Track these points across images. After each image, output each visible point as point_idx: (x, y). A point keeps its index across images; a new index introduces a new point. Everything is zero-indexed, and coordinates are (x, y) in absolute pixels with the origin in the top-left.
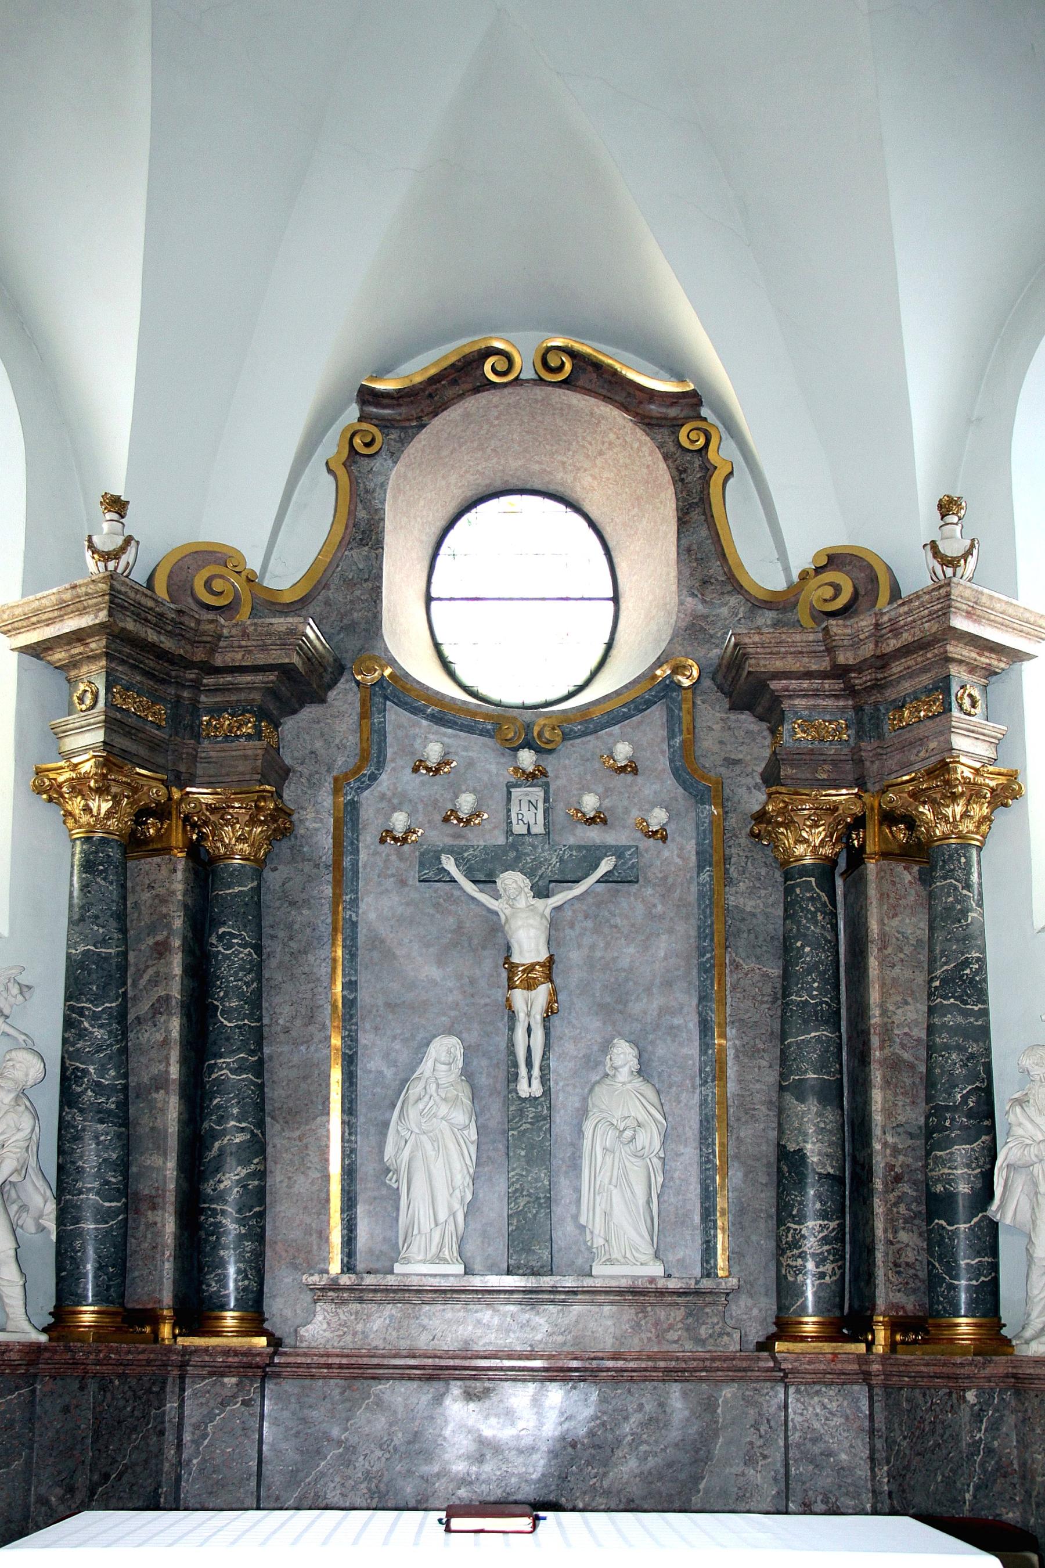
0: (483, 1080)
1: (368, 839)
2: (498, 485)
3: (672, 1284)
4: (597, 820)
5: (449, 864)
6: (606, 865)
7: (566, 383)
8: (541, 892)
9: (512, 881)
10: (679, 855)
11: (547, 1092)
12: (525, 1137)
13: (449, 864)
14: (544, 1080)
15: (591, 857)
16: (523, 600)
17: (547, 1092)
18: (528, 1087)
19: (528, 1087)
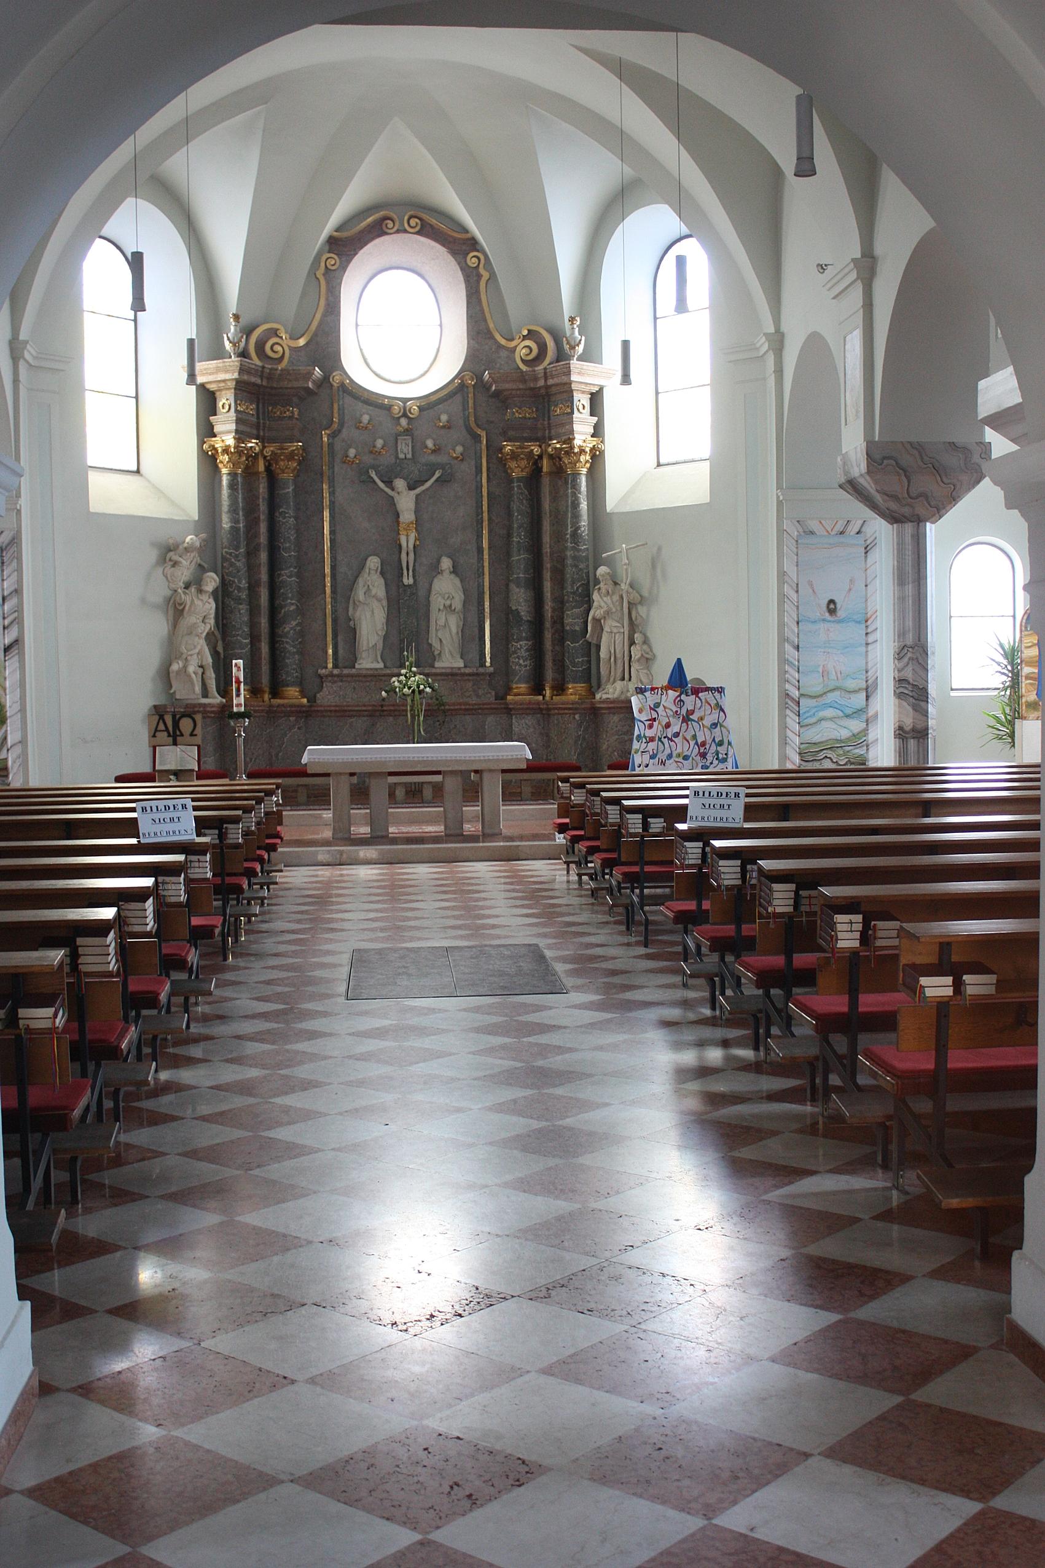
1: (338, 460)
2: (388, 266)
3: (467, 671)
5: (373, 475)
6: (437, 475)
7: (418, 233)
9: (400, 484)
13: (373, 475)
14: (414, 577)
15: (431, 469)
16: (401, 335)
18: (408, 580)
19: (408, 580)
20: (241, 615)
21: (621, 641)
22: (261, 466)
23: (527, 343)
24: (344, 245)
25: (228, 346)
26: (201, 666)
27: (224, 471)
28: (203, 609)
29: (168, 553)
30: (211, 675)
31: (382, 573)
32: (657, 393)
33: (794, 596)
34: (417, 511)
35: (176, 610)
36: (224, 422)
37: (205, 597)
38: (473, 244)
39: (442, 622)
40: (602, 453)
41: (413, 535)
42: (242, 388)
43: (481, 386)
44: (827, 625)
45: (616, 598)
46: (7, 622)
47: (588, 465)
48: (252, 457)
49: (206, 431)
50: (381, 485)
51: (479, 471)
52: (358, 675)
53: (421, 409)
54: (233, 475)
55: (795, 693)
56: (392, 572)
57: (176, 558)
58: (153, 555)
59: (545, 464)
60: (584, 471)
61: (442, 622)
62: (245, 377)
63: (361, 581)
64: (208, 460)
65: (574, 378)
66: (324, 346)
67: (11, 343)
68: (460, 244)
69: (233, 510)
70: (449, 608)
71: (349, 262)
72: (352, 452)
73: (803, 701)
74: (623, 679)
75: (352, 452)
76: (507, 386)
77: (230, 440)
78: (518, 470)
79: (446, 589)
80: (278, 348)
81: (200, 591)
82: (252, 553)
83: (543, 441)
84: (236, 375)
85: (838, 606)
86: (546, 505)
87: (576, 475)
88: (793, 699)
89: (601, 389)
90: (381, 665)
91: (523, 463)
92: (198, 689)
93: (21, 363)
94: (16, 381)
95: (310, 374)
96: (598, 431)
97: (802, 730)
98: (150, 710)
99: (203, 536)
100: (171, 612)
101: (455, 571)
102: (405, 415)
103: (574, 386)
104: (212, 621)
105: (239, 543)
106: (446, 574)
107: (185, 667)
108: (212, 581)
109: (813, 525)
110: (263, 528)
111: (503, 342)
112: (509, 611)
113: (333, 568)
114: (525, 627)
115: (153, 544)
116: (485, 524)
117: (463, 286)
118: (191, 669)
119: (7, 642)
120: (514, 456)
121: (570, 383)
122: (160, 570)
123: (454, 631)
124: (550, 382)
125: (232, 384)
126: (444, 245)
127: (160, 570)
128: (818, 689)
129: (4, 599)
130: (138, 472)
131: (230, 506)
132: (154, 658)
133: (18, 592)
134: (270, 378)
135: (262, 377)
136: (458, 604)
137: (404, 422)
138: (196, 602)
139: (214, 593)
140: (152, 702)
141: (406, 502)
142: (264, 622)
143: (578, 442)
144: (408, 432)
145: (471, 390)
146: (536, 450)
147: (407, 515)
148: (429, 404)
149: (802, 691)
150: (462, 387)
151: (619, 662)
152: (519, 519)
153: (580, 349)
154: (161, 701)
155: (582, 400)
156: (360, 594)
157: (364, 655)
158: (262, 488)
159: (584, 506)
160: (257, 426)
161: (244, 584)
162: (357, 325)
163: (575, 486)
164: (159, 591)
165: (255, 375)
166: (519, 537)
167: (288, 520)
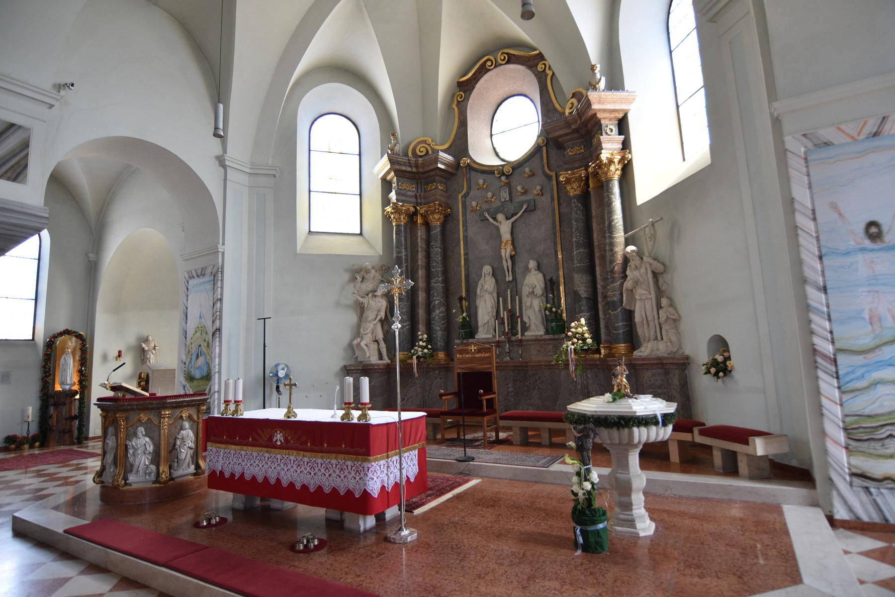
1: (468, 211)
2: (505, 96)
3: (547, 337)
4: (525, 192)
7: (508, 63)
8: (507, 218)
9: (500, 217)
10: (544, 201)
11: (514, 279)
17: (514, 279)
21: (650, 305)
22: (420, 220)
24: (465, 87)
26: (377, 341)
29: (357, 273)
30: (383, 345)
32: (678, 107)
33: (811, 225)
34: (512, 233)
35: (361, 309)
37: (377, 299)
38: (541, 57)
39: (528, 304)
40: (630, 161)
41: (509, 248)
44: (869, 256)
45: (643, 270)
47: (619, 172)
49: (386, 201)
50: (491, 220)
54: (397, 226)
55: (829, 349)
58: (346, 277)
60: (616, 177)
61: (528, 304)
62: (397, 167)
64: (386, 218)
65: (595, 106)
66: (460, 146)
68: (532, 61)
71: (470, 94)
72: (474, 204)
73: (841, 359)
74: (656, 339)
76: (558, 134)
78: (574, 190)
79: (534, 281)
80: (422, 149)
85: (885, 228)
87: (609, 181)
88: (825, 357)
91: (575, 185)
93: (229, 171)
95: (436, 160)
96: (626, 145)
97: (845, 397)
100: (358, 309)
101: (539, 268)
102: (503, 174)
103: (599, 115)
104: (382, 314)
106: (533, 272)
109: (827, 134)
110: (421, 256)
112: (576, 294)
113: (467, 276)
114: (584, 302)
115: (346, 270)
116: (558, 234)
120: (568, 181)
123: (537, 309)
127: (352, 285)
128: (867, 341)
130: (361, 234)
133: (221, 300)
135: (411, 166)
136: (539, 290)
137: (503, 178)
138: (372, 303)
140: (343, 363)
141: (505, 228)
143: (604, 156)
145: (544, 148)
148: (517, 166)
149: (838, 345)
151: (651, 324)
153: (602, 85)
155: (609, 126)
157: (480, 329)
158: (421, 233)
160: (416, 196)
162: (491, 135)
164: (350, 295)
165: (405, 165)
167: (437, 250)
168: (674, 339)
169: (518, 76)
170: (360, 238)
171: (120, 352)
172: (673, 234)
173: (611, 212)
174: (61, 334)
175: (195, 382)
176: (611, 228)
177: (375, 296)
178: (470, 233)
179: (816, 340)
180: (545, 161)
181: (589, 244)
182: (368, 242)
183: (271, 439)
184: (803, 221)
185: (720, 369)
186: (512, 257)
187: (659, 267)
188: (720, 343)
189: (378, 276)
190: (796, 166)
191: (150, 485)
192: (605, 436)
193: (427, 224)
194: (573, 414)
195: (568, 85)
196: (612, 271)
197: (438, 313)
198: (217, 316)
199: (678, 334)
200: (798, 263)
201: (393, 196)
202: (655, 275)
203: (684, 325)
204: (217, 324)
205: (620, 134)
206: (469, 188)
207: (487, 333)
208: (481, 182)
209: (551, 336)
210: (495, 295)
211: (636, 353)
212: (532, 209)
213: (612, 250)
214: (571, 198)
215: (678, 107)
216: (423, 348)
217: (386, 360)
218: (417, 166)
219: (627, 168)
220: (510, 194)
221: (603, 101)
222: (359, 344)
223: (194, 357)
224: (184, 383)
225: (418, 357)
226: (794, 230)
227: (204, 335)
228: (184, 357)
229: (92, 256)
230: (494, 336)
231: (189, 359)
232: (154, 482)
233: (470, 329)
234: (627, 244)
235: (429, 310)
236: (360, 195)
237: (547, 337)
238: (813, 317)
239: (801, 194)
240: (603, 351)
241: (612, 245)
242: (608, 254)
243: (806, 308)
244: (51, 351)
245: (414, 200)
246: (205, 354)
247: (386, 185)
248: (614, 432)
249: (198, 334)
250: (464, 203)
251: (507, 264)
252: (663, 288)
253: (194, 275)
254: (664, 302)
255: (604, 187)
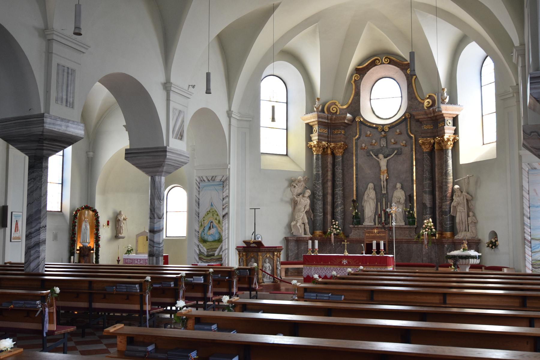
0: (377, 191)
1: (359, 148)
3: (406, 226)
4: (396, 143)
5: (371, 153)
7: (388, 64)
8: (385, 157)
9: (381, 156)
10: (407, 150)
11: (387, 192)
12: (383, 199)
13: (371, 153)
14: (387, 190)
15: (393, 150)
16: (384, 101)
17: (387, 192)
18: (384, 192)
20: (319, 205)
21: (464, 215)
22: (329, 152)
23: (428, 100)
24: (361, 71)
25: (315, 109)
26: (304, 223)
27: (315, 153)
28: (305, 202)
29: (292, 183)
30: (307, 226)
31: (375, 189)
32: (482, 116)
33: (527, 196)
35: (295, 204)
36: (315, 136)
37: (305, 199)
40: (458, 141)
41: (386, 175)
42: (320, 123)
43: (412, 116)
45: (462, 198)
46: (224, 207)
47: (452, 146)
48: (325, 149)
49: (309, 139)
50: (374, 157)
51: (412, 150)
52: (365, 228)
53: (389, 128)
54: (317, 155)
55: (529, 238)
56: (377, 189)
57: (295, 185)
58: (286, 184)
59: (436, 146)
60: (450, 148)
62: (320, 120)
63: (366, 193)
64: (309, 149)
66: (355, 107)
67: (227, 112)
69: (317, 167)
70: (399, 202)
71: (363, 77)
72: (363, 145)
73: (532, 241)
74: (466, 231)
75: (363, 145)
77: (315, 143)
78: (426, 149)
79: (399, 194)
80: (334, 109)
81: (304, 196)
82: (324, 184)
83: (434, 137)
84: (317, 119)
86: (437, 162)
87: (447, 150)
88: (528, 241)
89: (457, 116)
90: (373, 224)
91: (427, 146)
92: (302, 231)
93: (232, 120)
94: (230, 125)
95: (345, 118)
96: (456, 132)
97: (533, 254)
98: (283, 239)
99: (306, 177)
100: (293, 204)
101: (402, 188)
102: (383, 131)
103: (444, 115)
104: (308, 208)
105: (319, 179)
106: (399, 190)
107: (296, 223)
108: (308, 193)
110: (330, 174)
111: (420, 100)
113: (357, 188)
114: (428, 210)
115: (286, 180)
117: (406, 81)
118: (298, 224)
119: (224, 213)
120: (423, 143)
121: (443, 114)
122: (289, 189)
124: (436, 114)
125: (316, 123)
126: (398, 67)
129: (223, 199)
130: (287, 155)
131: (316, 166)
132: (285, 220)
133: (228, 196)
134: (331, 120)
135: (328, 119)
138: (302, 200)
139: (309, 197)
140: (284, 236)
141: (383, 163)
142: (329, 208)
143: (446, 137)
144: (385, 137)
145: (409, 120)
146: (432, 141)
147: (384, 167)
148: (392, 126)
149: (532, 237)
150: (405, 119)
151: (464, 223)
152: (427, 168)
153: (447, 100)
154: (288, 235)
155: (449, 121)
156: (365, 197)
157: (366, 220)
158: (330, 159)
159: (450, 162)
160: (328, 137)
161: (321, 194)
162: (370, 99)
163: (446, 154)
164: (288, 195)
166: (427, 175)
167: (339, 171)
168: (474, 231)
169: (393, 70)
170: (285, 158)
171: (108, 222)
172: (477, 183)
173: (447, 166)
174: (83, 209)
175: (208, 243)
176: (446, 174)
177: (304, 196)
178: (360, 162)
179: (526, 235)
180: (409, 127)
181: (432, 179)
182: (293, 161)
183: (341, 262)
184: (525, 194)
185: (493, 245)
186: (386, 180)
187: (469, 197)
188: (494, 234)
189: (304, 185)
190: (525, 174)
191: (271, 283)
192: (461, 261)
193: (333, 154)
194: (449, 256)
195: (426, 89)
196: (446, 196)
197: (339, 209)
198: (226, 206)
199: (476, 229)
200: (522, 208)
201: (315, 137)
202: (467, 201)
203: (479, 225)
204: (226, 211)
205: (454, 126)
206: (360, 135)
207: (370, 222)
208: (369, 133)
209: (409, 226)
210: (375, 201)
211: (456, 237)
212: (399, 153)
213: (446, 185)
214: (423, 153)
215: (482, 116)
216: (336, 229)
217: (309, 235)
218: (331, 120)
219: (456, 143)
220: (387, 142)
221: (447, 110)
222: (295, 225)
223: (207, 229)
224: (197, 243)
225: (334, 234)
226: (522, 196)
227: (215, 216)
228: (197, 228)
229: (91, 154)
230: (375, 224)
231: (202, 230)
232: (272, 282)
233: (358, 219)
234: (454, 183)
235: (333, 207)
236: (287, 129)
237: (406, 226)
238: (525, 227)
239: (525, 185)
240: (437, 235)
241: (447, 183)
242: (444, 187)
243: (523, 224)
244: (75, 219)
245: (326, 139)
246: (216, 227)
247: (309, 128)
248: (464, 260)
249: (210, 215)
250: (356, 143)
251: (383, 184)
252: (471, 207)
253: (205, 179)
254: (471, 214)
255: (443, 151)
